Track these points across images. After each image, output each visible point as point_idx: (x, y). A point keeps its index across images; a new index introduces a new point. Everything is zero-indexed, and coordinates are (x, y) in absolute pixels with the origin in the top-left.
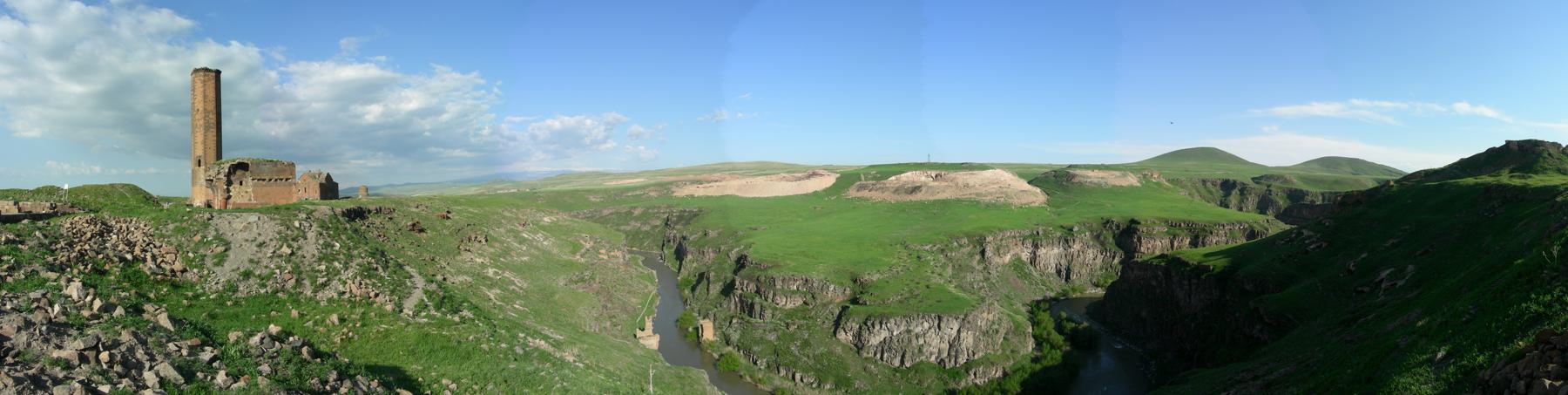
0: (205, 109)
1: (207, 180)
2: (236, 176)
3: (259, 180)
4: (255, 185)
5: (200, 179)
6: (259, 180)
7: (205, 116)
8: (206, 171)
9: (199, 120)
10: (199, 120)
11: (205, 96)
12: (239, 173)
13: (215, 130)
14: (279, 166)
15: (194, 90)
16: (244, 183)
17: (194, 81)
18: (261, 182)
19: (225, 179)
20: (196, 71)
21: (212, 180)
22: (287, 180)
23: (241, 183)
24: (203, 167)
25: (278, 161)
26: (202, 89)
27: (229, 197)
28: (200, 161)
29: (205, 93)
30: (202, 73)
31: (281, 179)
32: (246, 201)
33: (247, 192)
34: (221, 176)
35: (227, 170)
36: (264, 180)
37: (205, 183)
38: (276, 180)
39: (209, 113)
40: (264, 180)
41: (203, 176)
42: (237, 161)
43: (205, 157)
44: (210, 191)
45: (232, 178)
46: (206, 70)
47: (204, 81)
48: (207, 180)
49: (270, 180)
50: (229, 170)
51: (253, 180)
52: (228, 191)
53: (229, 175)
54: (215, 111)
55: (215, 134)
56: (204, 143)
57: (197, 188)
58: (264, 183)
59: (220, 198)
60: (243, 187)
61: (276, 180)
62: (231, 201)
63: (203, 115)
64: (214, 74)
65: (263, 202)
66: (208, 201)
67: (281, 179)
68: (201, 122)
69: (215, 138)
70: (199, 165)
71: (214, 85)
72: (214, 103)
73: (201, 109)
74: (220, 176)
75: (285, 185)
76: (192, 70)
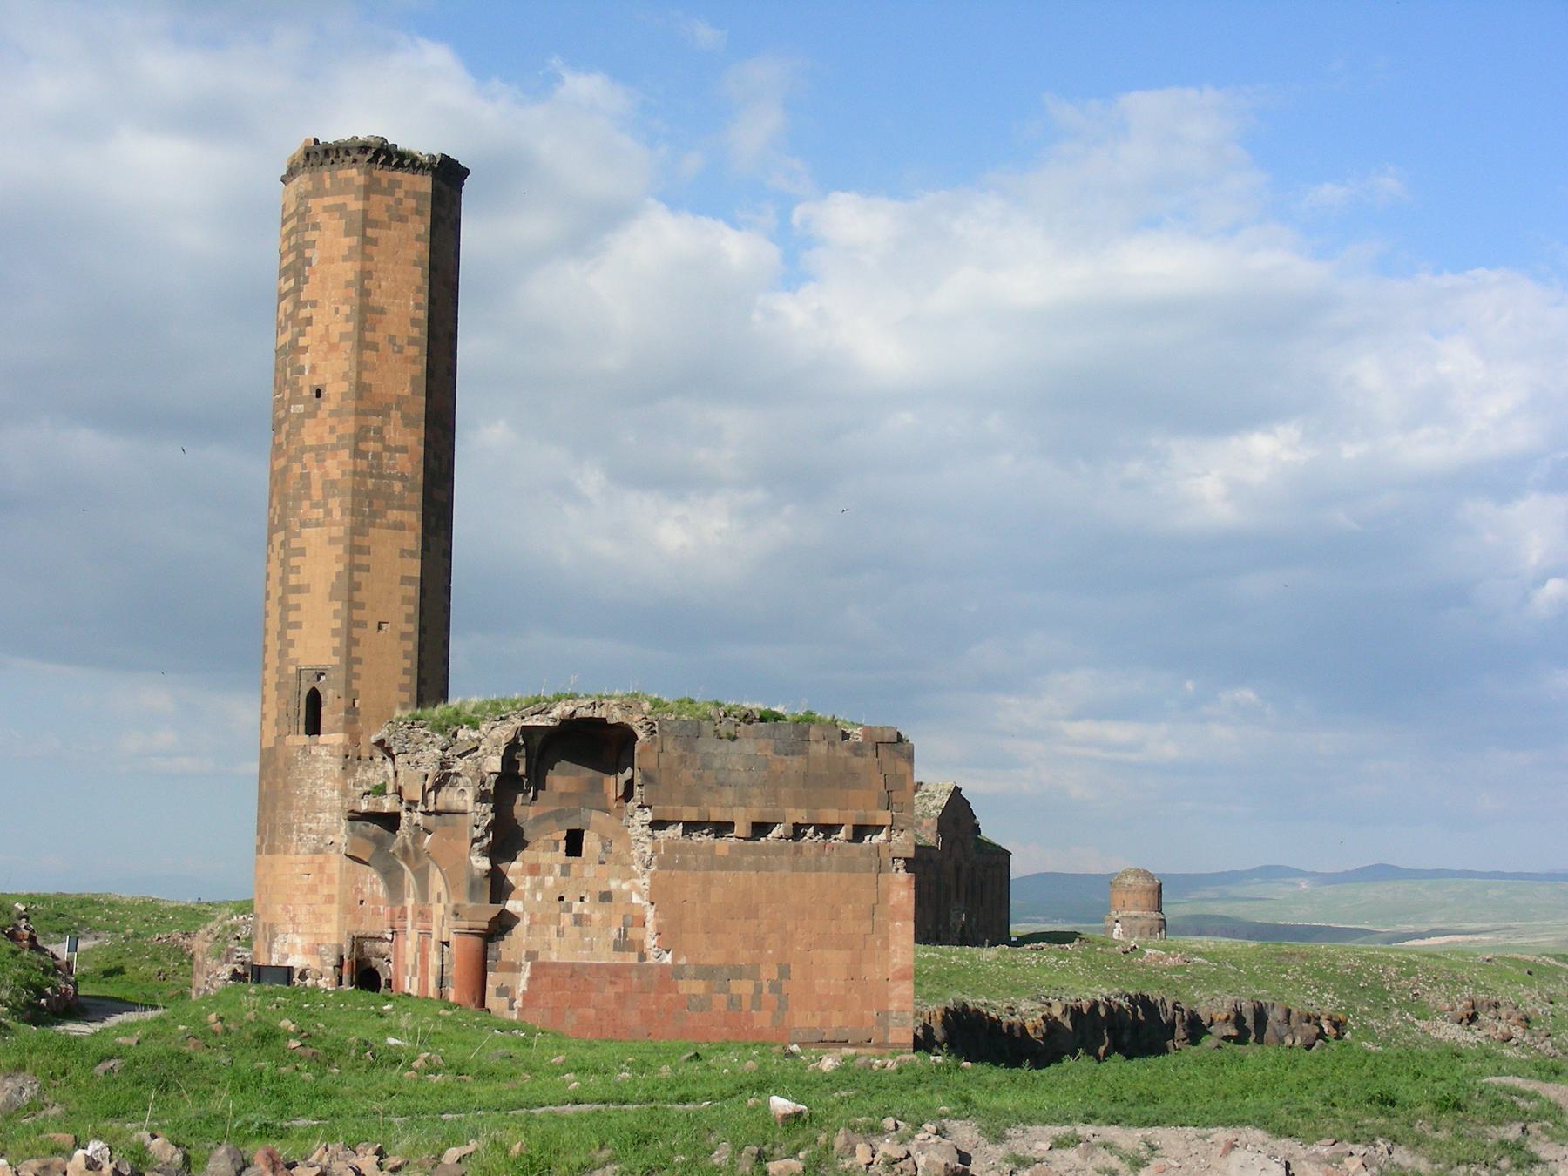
0: (361, 390)
1: (356, 817)
2: (547, 802)
3: (690, 827)
4: (666, 861)
5: (313, 807)
6: (690, 827)
7: (361, 435)
8: (350, 760)
9: (320, 451)
10: (320, 451)
11: (367, 314)
12: (564, 779)
13: (413, 518)
14: (819, 749)
15: (296, 268)
16: (590, 842)
17: (299, 221)
18: (703, 839)
19: (484, 814)
20: (319, 155)
21: (390, 821)
22: (860, 832)
23: (574, 844)
24: (332, 738)
25: (809, 719)
26: (349, 270)
27: (502, 925)
28: (314, 701)
29: (364, 293)
30: (354, 174)
31: (829, 830)
32: (608, 957)
33: (606, 897)
34: (462, 797)
35: (495, 764)
36: (722, 828)
37: (341, 835)
38: (797, 831)
39: (384, 412)
40: (722, 828)
41: (330, 795)
42: (560, 711)
43: (351, 677)
44: (372, 883)
45: (524, 810)
46: (383, 155)
47: (367, 221)
48: (356, 817)
49: (760, 829)
50: (508, 760)
51: (658, 824)
52: (499, 888)
53: (503, 791)
54: (419, 406)
55: (412, 539)
56: (350, 590)
57: (293, 864)
58: (724, 845)
59: (443, 926)
60: (587, 867)
61: (797, 831)
62: (511, 947)
63: (349, 426)
64: (425, 184)
65: (714, 958)
66: (358, 942)
67: (829, 830)
68: (337, 466)
69: (414, 568)
70: (313, 727)
71: (421, 250)
72: (417, 352)
73: (337, 389)
74: (449, 797)
75: (848, 866)
76: (294, 146)
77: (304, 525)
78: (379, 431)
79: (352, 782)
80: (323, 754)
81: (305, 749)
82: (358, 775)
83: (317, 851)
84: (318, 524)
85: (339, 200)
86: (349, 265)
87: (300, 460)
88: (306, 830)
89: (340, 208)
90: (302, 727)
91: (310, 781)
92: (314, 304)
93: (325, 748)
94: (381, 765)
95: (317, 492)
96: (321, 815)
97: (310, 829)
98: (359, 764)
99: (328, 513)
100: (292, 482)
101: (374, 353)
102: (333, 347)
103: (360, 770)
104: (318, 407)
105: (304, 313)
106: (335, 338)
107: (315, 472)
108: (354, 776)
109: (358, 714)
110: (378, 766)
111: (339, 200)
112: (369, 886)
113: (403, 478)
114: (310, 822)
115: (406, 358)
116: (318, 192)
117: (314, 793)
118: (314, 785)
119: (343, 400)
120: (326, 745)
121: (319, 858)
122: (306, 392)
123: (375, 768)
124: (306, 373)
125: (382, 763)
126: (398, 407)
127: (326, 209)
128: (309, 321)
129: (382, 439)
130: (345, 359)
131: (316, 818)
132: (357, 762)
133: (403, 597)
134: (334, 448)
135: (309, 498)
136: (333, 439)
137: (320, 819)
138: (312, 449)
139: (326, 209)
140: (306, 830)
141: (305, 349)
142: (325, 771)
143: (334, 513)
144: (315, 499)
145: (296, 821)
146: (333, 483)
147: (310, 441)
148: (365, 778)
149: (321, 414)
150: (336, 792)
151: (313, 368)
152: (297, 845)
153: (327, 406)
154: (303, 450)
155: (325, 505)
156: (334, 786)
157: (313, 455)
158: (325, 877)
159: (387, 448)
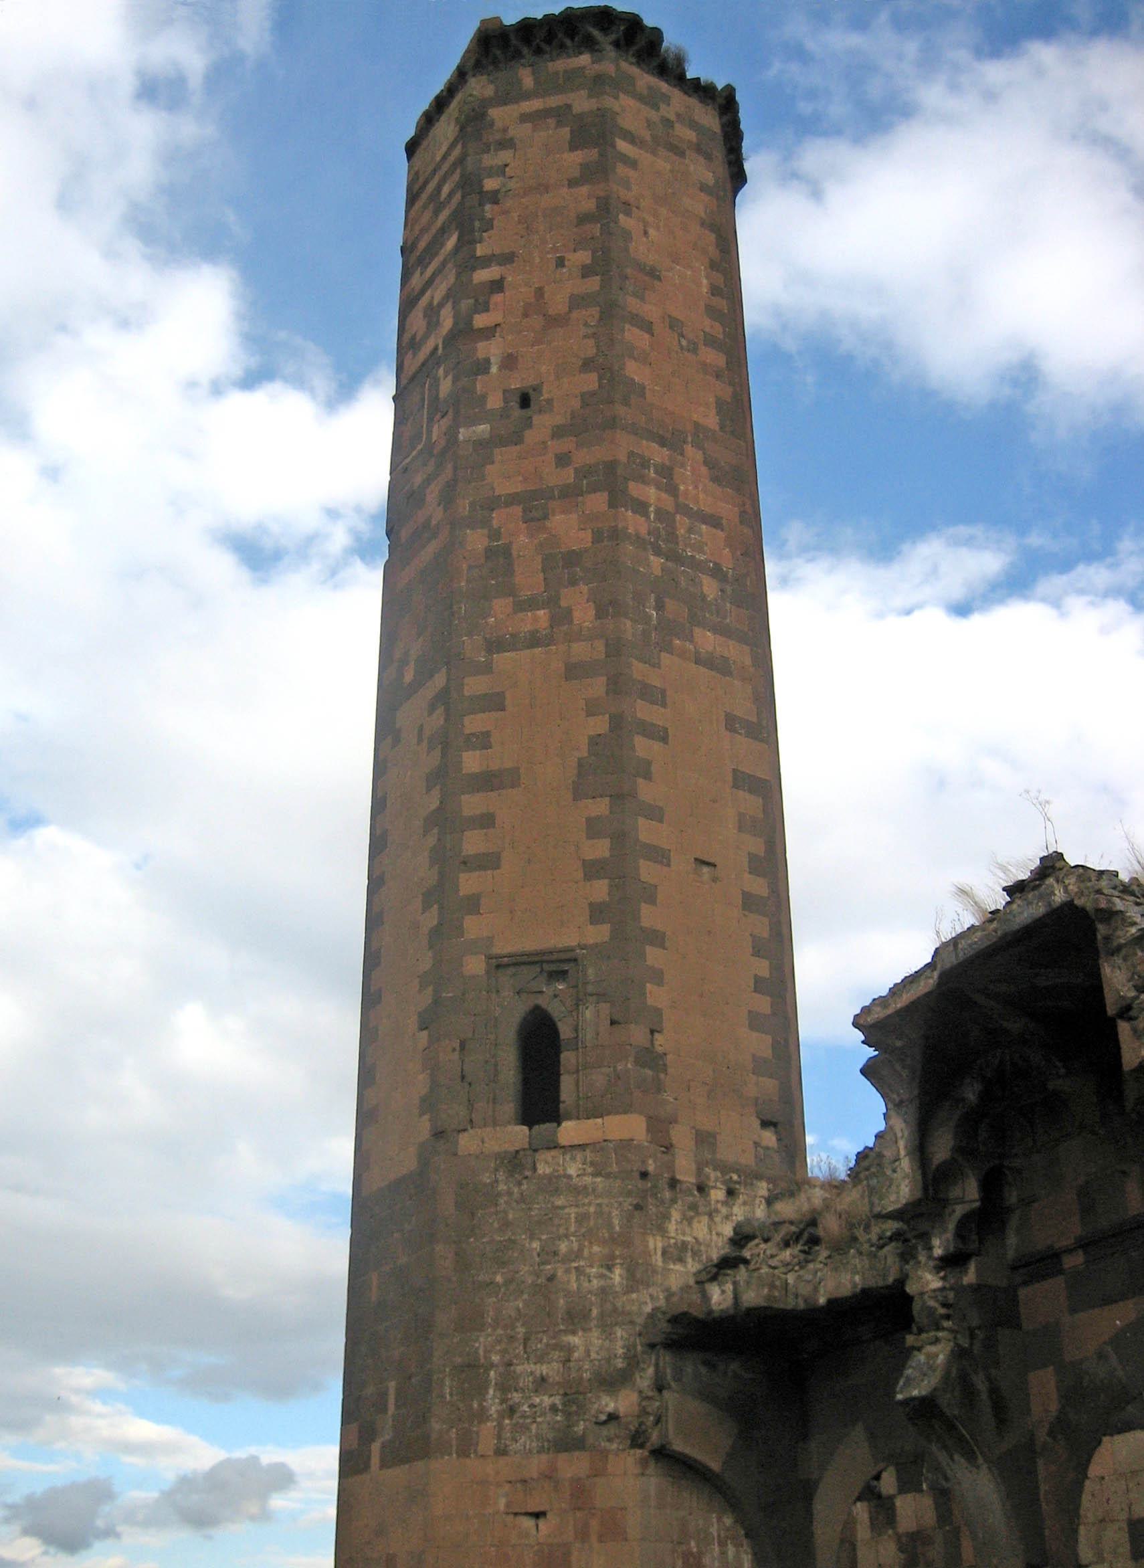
77: (496, 645)
78: (666, 472)
79: (660, 1245)
80: (572, 1171)
81: (515, 1163)
82: (672, 1227)
83: (566, 1443)
84: (534, 641)
85: (554, 101)
86: (585, 189)
87: (486, 523)
88: (526, 1382)
89: (561, 115)
90: (509, 1108)
91: (536, 1245)
92: (507, 259)
93: (579, 1155)
94: (724, 1210)
95: (528, 578)
96: (575, 1340)
97: (543, 1379)
98: (673, 1201)
99: (561, 617)
100: (465, 566)
101: (647, 336)
102: (554, 321)
103: (675, 1215)
104: (528, 423)
105: (483, 275)
106: (558, 302)
107: (523, 542)
108: (662, 1230)
109: (665, 1071)
110: (717, 1211)
111: (554, 101)
112: (717, 1548)
113: (717, 572)
114: (540, 1360)
115: (704, 364)
116: (503, 99)
117: (551, 1278)
118: (549, 1253)
119: (585, 404)
120: (582, 1147)
121: (573, 1466)
122: (495, 402)
123: (710, 1215)
124: (494, 369)
125: (725, 1203)
126: (698, 446)
127: (524, 118)
128: (497, 286)
129: (672, 490)
130: (585, 337)
131: (556, 1347)
132: (667, 1195)
133: (741, 816)
134: (570, 494)
135: (511, 592)
136: (568, 476)
137: (570, 1349)
138: (513, 499)
139: (524, 118)
140: (526, 1382)
141: (489, 332)
142: (582, 1218)
143: (577, 615)
144: (525, 594)
145: (495, 1358)
146: (572, 558)
147: (505, 488)
148: (688, 1239)
149: (531, 436)
150: (618, 1271)
151: (510, 362)
152: (500, 1426)
153: (543, 423)
154: (492, 504)
155: (551, 602)
156: (612, 1257)
157: (518, 510)
158: (594, 1524)
159: (685, 510)
